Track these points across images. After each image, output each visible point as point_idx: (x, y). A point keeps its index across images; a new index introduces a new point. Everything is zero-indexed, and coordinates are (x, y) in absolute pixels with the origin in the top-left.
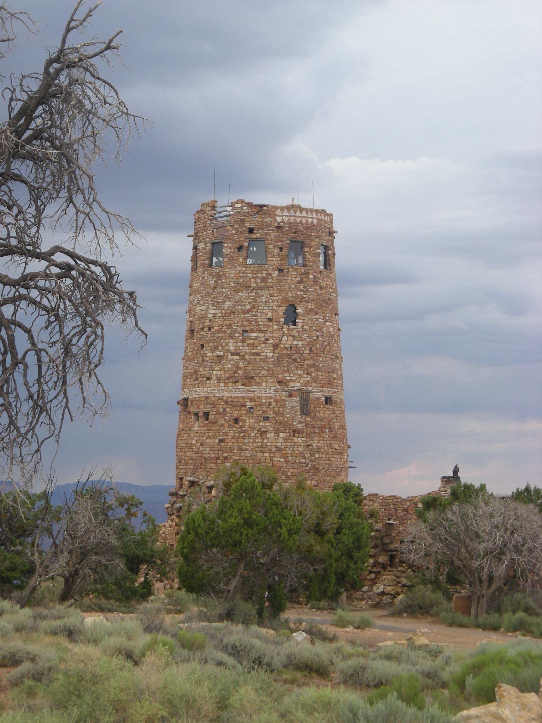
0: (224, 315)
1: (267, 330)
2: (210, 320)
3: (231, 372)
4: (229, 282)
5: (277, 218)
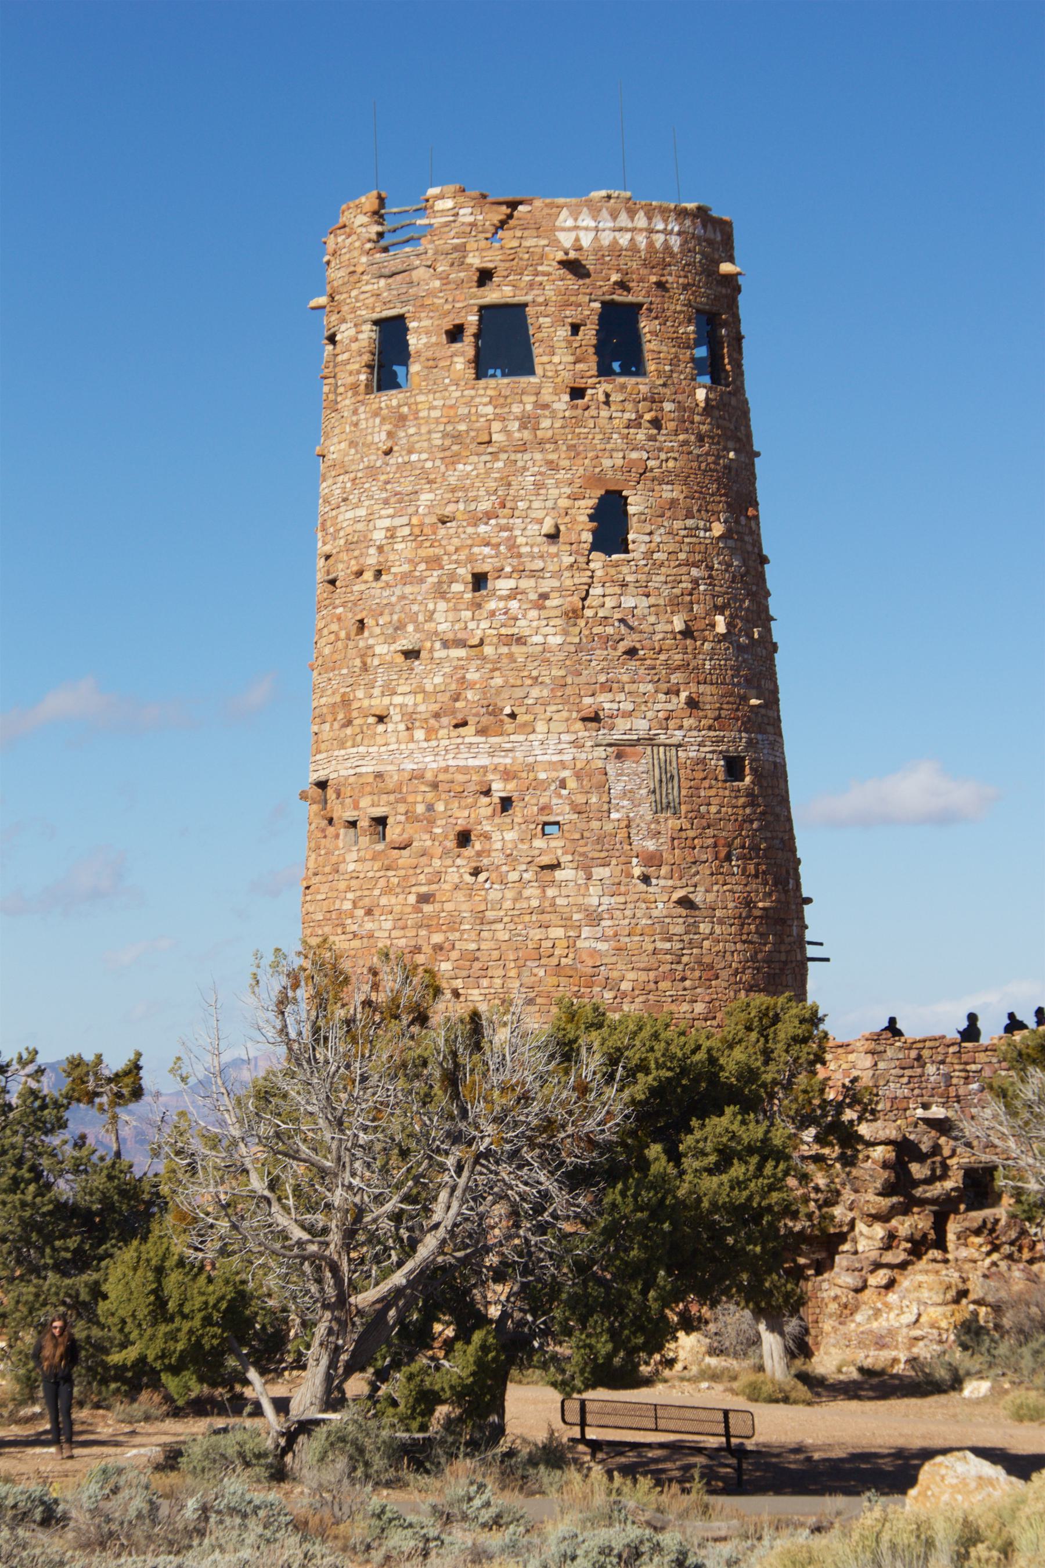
0: (417, 531)
2: (380, 549)
3: (445, 698)
4: (429, 432)
5: (561, 236)
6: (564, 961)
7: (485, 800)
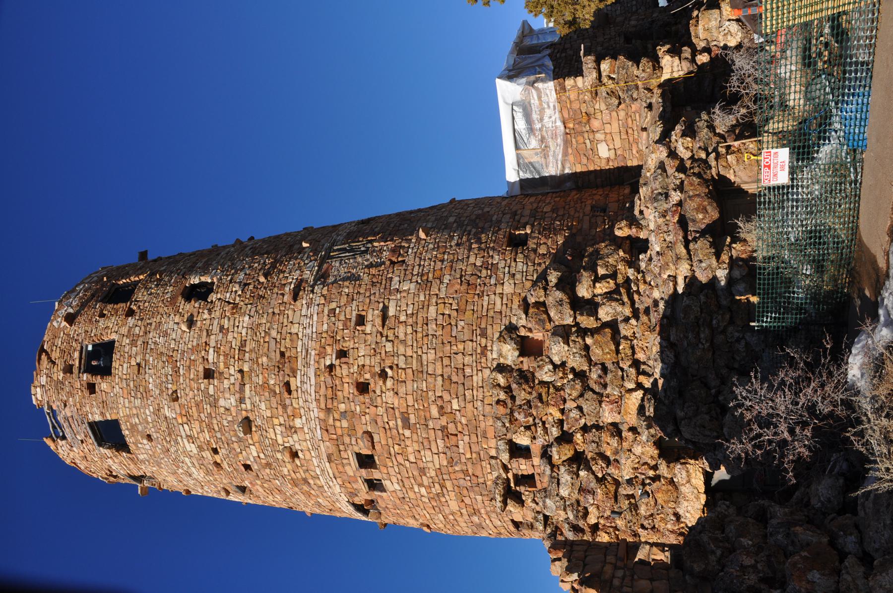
1: (207, 331)
6: (455, 307)
7: (338, 371)
